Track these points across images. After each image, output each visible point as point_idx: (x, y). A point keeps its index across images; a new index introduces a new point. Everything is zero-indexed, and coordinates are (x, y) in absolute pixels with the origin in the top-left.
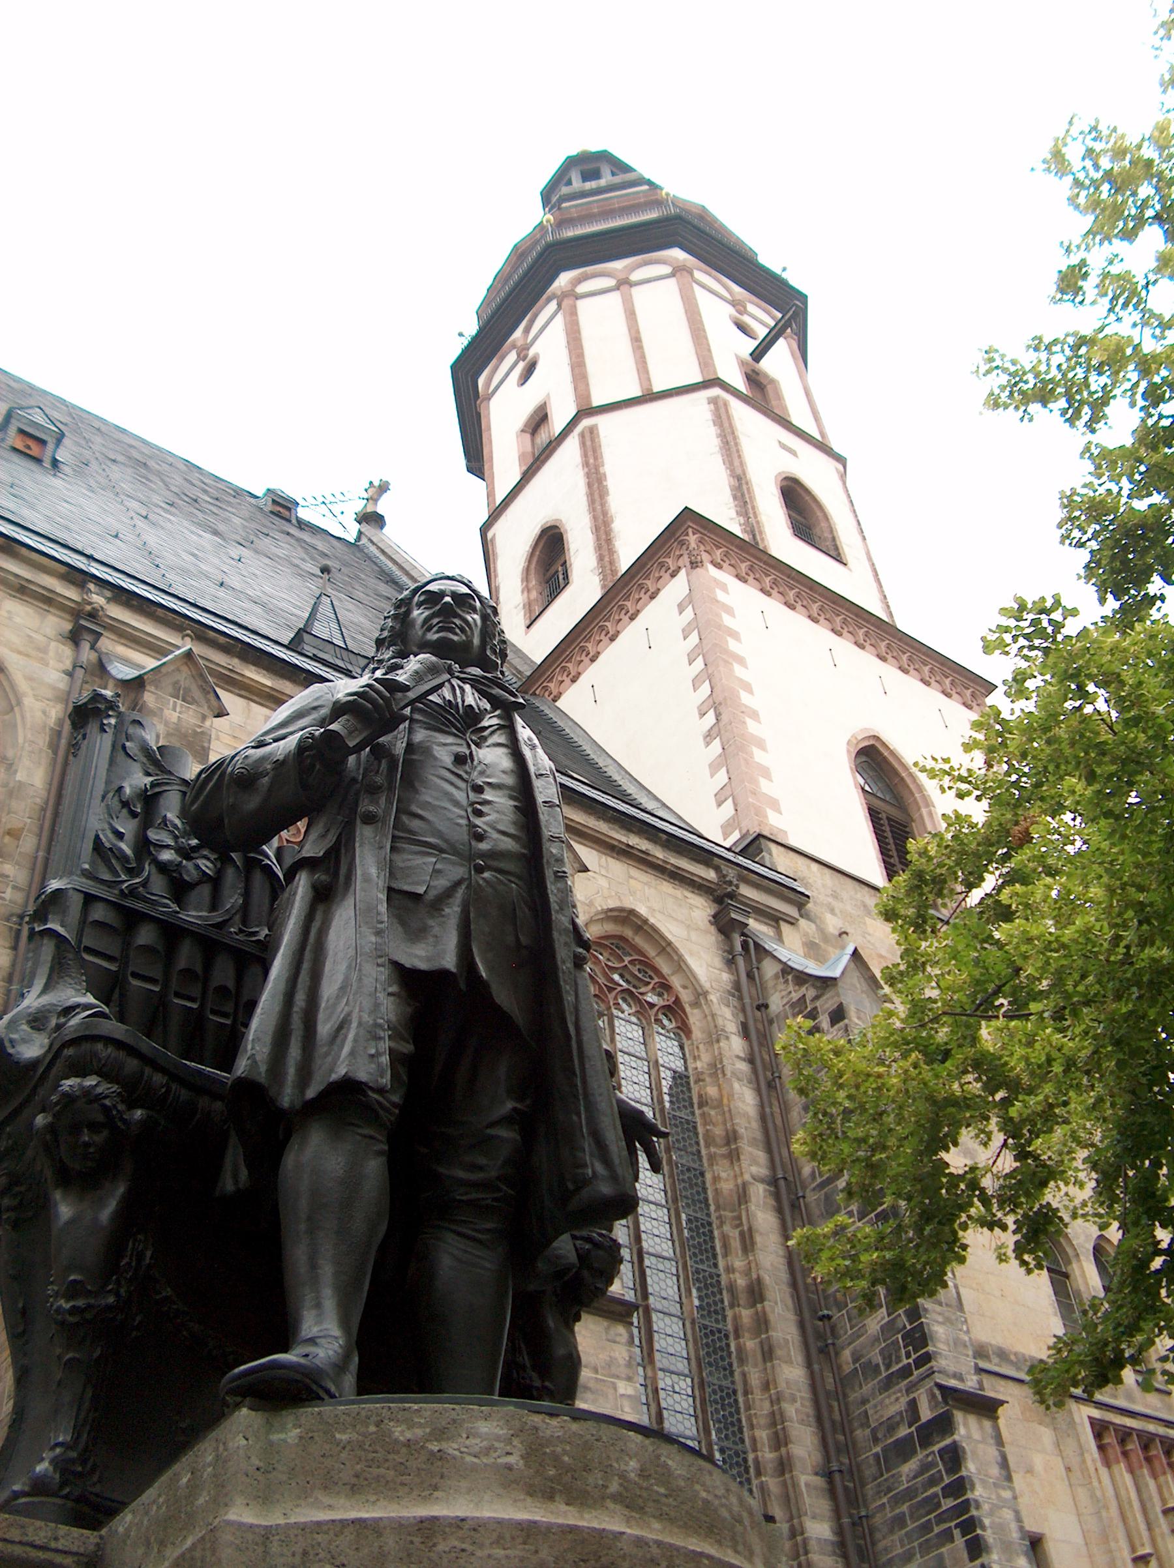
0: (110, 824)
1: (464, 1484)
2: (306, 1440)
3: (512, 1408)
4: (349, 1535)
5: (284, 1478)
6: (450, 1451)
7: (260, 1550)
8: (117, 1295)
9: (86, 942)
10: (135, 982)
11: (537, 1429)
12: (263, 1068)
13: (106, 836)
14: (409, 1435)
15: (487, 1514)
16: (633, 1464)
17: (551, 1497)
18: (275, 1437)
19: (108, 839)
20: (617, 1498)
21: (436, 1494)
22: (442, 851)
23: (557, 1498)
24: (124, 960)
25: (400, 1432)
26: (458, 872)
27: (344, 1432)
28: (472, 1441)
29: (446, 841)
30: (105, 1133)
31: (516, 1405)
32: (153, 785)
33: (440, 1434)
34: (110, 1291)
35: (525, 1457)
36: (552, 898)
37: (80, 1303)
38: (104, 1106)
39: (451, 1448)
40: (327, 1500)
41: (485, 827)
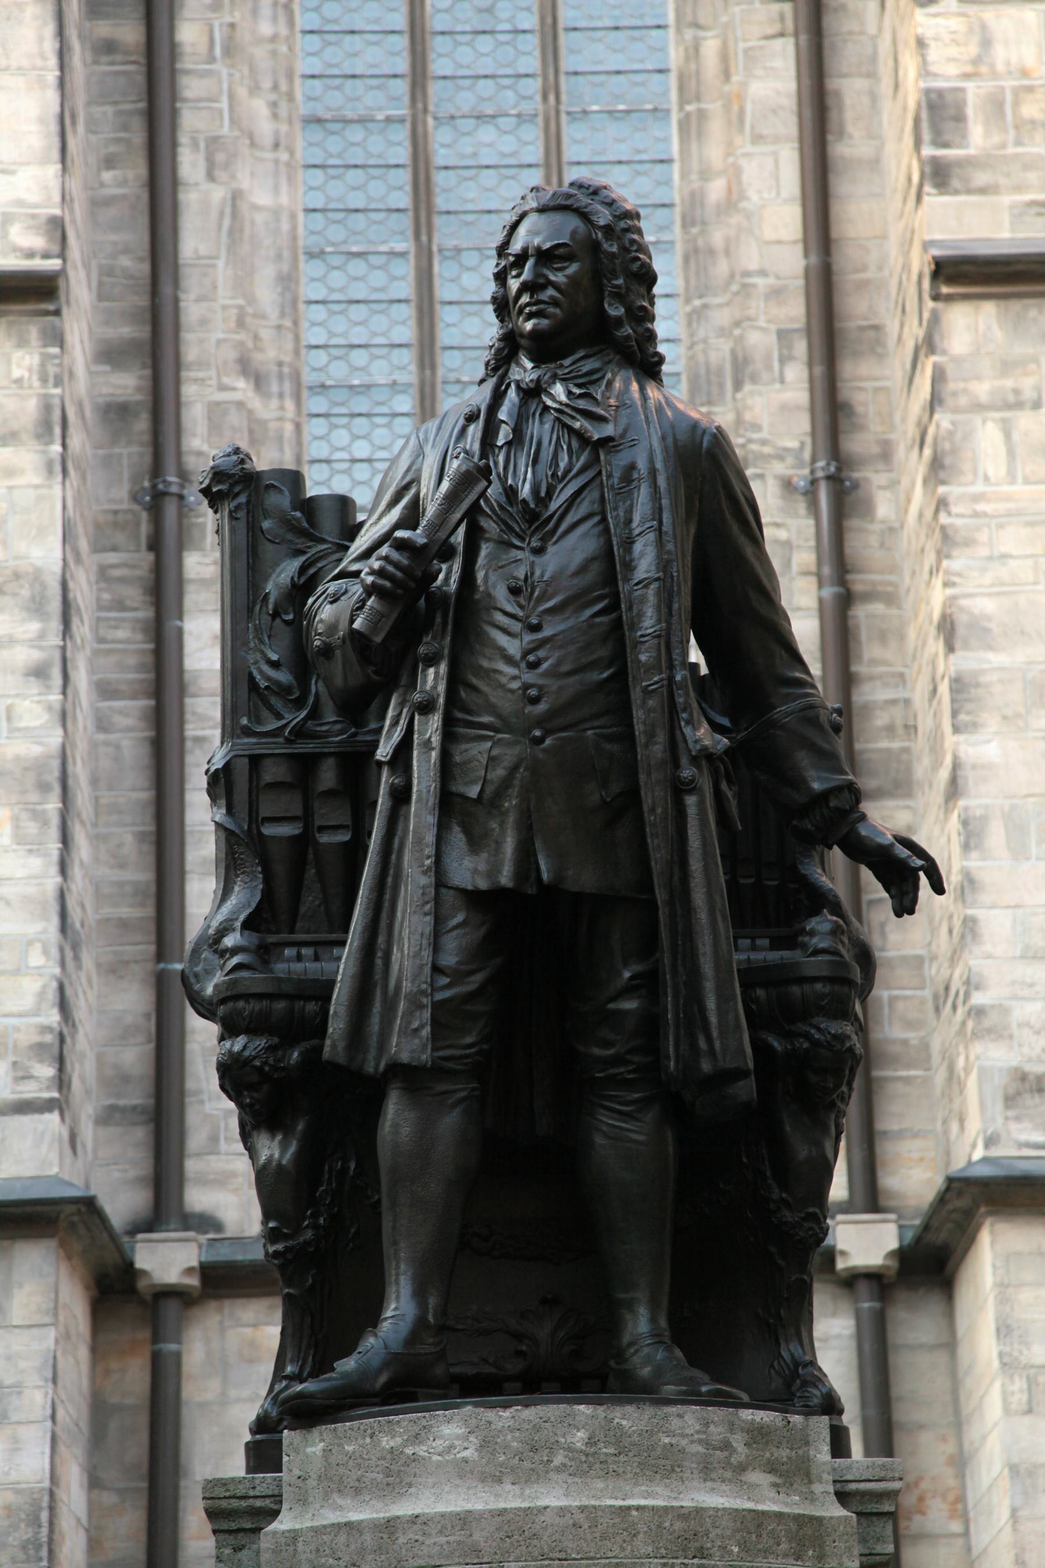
0: (262, 652)
1: (430, 1480)
2: (327, 1451)
3: (469, 1408)
4: (342, 1538)
5: (315, 1483)
6: (422, 1453)
7: (291, 1549)
8: (315, 1227)
9: (265, 812)
10: (324, 839)
11: (490, 1423)
12: (341, 1045)
13: (261, 672)
14: (392, 1444)
15: (441, 1508)
16: (581, 1435)
17: (500, 1481)
18: (309, 1450)
19: (264, 674)
20: (561, 1469)
21: (411, 1490)
22: (497, 731)
23: (504, 1479)
24: (307, 817)
25: (386, 1442)
26: (509, 755)
27: (349, 1445)
28: (438, 1442)
29: (499, 716)
30: (265, 1088)
31: (476, 1405)
32: (303, 570)
33: (416, 1438)
34: (307, 1227)
35: (481, 1448)
36: (639, 728)
37: (279, 1247)
38: (254, 1067)
39: (421, 1450)
40: (340, 1501)
41: (541, 682)
